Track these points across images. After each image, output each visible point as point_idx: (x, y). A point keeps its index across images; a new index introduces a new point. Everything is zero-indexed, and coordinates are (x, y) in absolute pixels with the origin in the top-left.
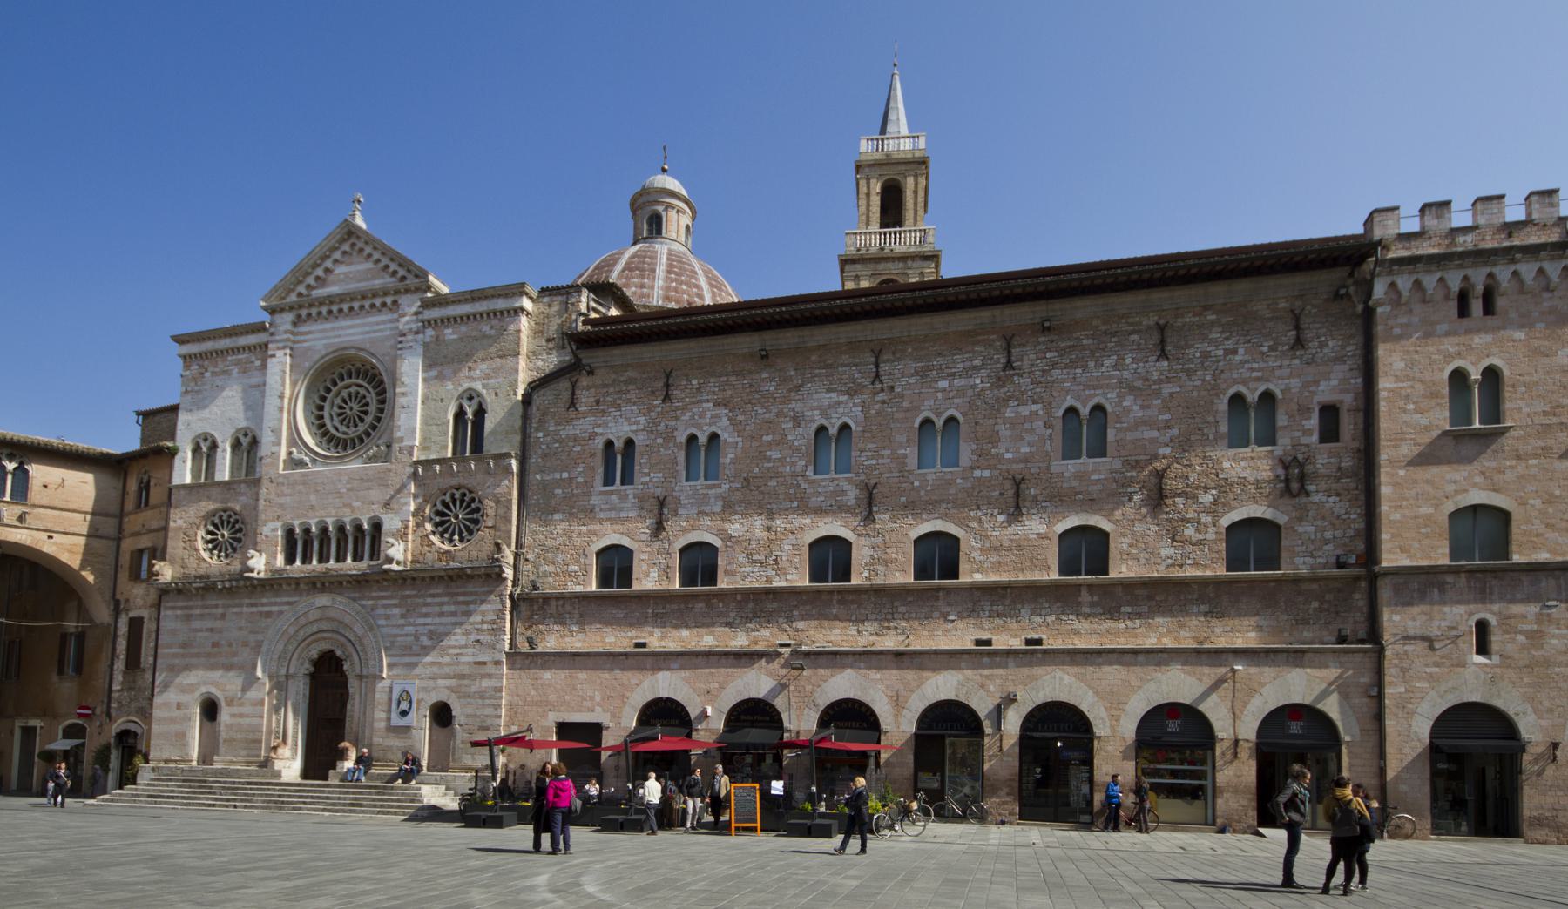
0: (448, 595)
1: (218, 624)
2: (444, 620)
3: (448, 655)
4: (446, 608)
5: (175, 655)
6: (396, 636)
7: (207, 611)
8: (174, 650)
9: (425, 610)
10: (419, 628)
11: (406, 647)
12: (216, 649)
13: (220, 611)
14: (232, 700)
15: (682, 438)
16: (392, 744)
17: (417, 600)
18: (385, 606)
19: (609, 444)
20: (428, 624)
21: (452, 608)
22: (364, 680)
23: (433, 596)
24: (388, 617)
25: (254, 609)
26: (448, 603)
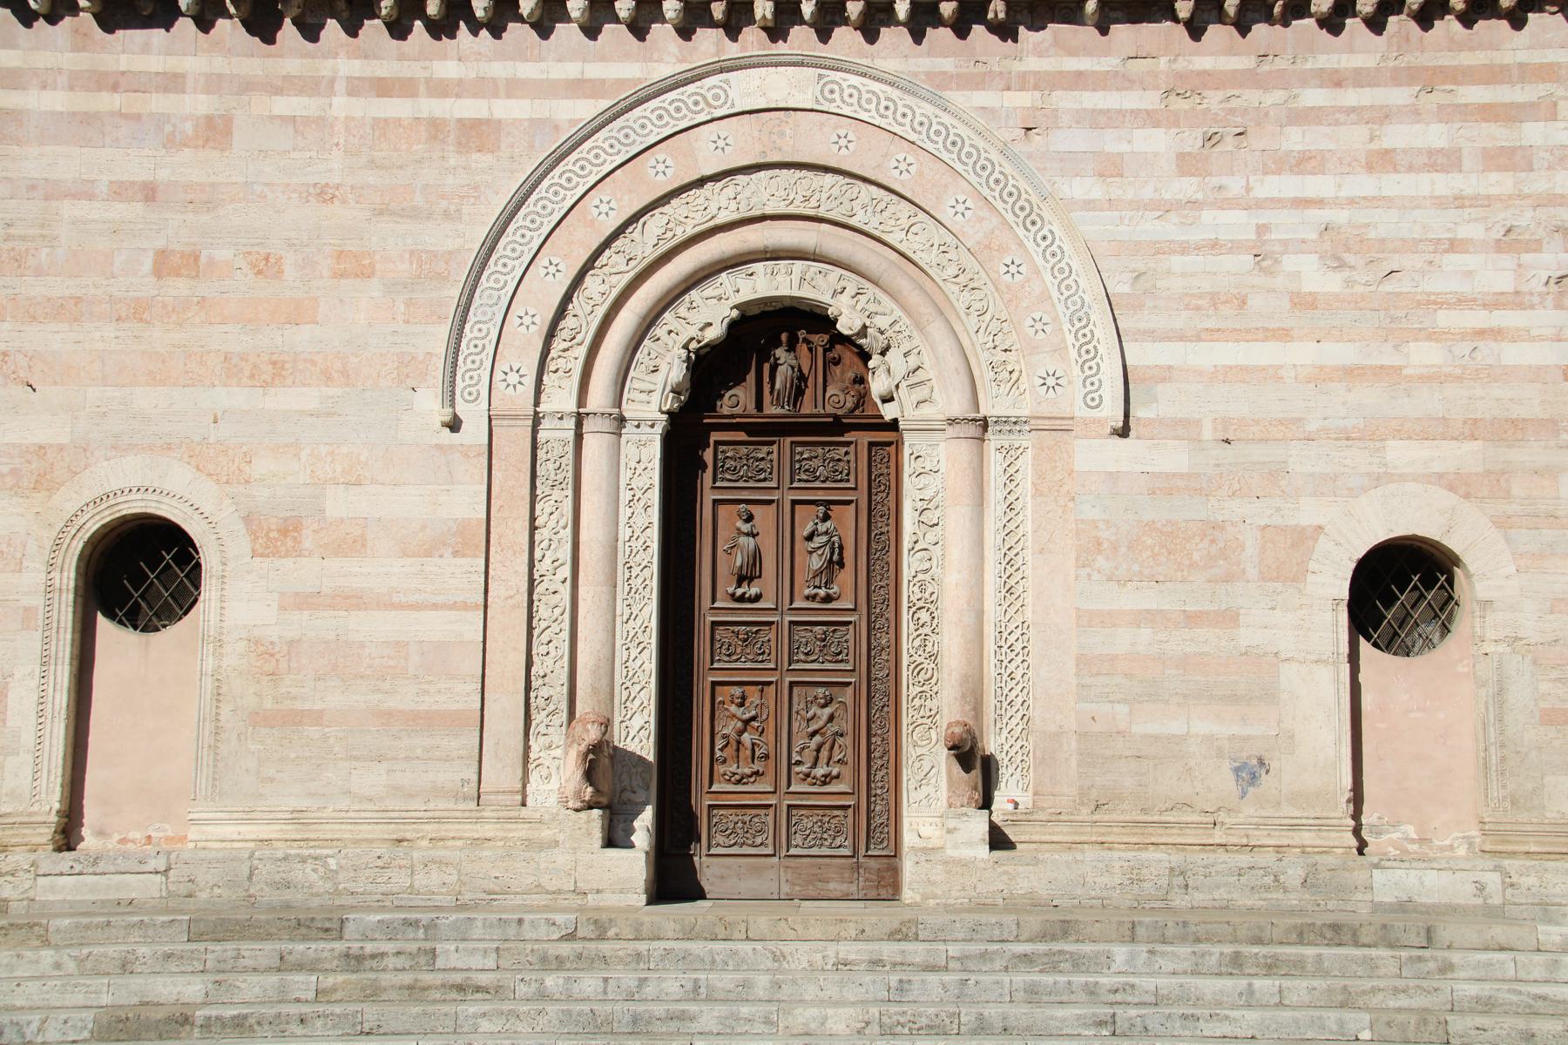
0: (1399, 77)
2: (1392, 184)
3: (1433, 336)
4: (1398, 136)
6: (1160, 249)
7: (108, 102)
9: (1295, 139)
10: (1266, 217)
11: (1215, 300)
12: (179, 287)
13: (198, 104)
14: (290, 528)
16: (1176, 727)
17: (1251, 97)
20: (1320, 203)
21: (1436, 135)
22: (993, 440)
23: (1336, 80)
24: (1110, 168)
25: (396, 108)
26: (1415, 114)
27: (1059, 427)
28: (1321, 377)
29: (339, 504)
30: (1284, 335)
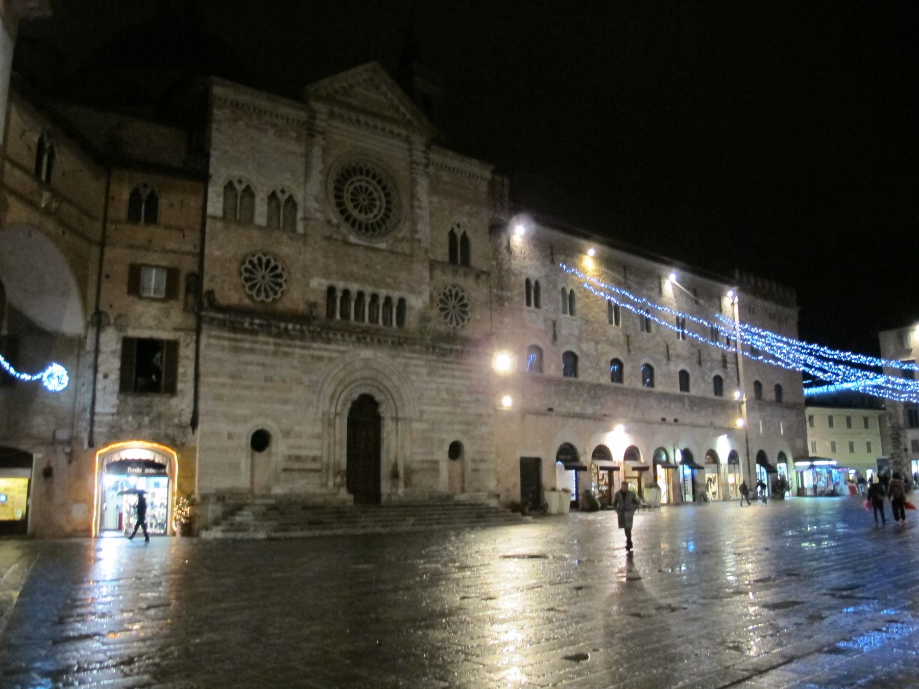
1: (269, 360)
5: (223, 385)
8: (221, 380)
9: (442, 372)
12: (268, 384)
15: (560, 288)
18: (416, 366)
19: (528, 282)
24: (417, 374)
25: (306, 352)
27: (411, 420)
28: (446, 413)
29: (297, 429)
30: (440, 405)
